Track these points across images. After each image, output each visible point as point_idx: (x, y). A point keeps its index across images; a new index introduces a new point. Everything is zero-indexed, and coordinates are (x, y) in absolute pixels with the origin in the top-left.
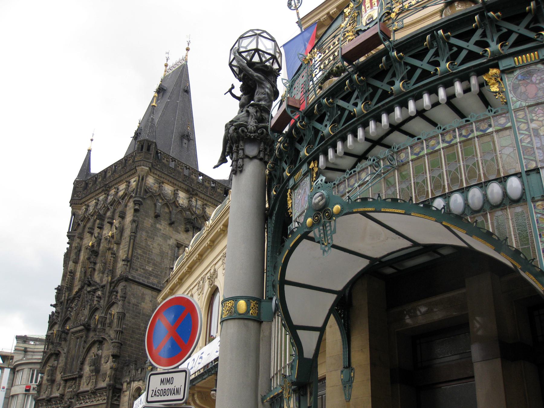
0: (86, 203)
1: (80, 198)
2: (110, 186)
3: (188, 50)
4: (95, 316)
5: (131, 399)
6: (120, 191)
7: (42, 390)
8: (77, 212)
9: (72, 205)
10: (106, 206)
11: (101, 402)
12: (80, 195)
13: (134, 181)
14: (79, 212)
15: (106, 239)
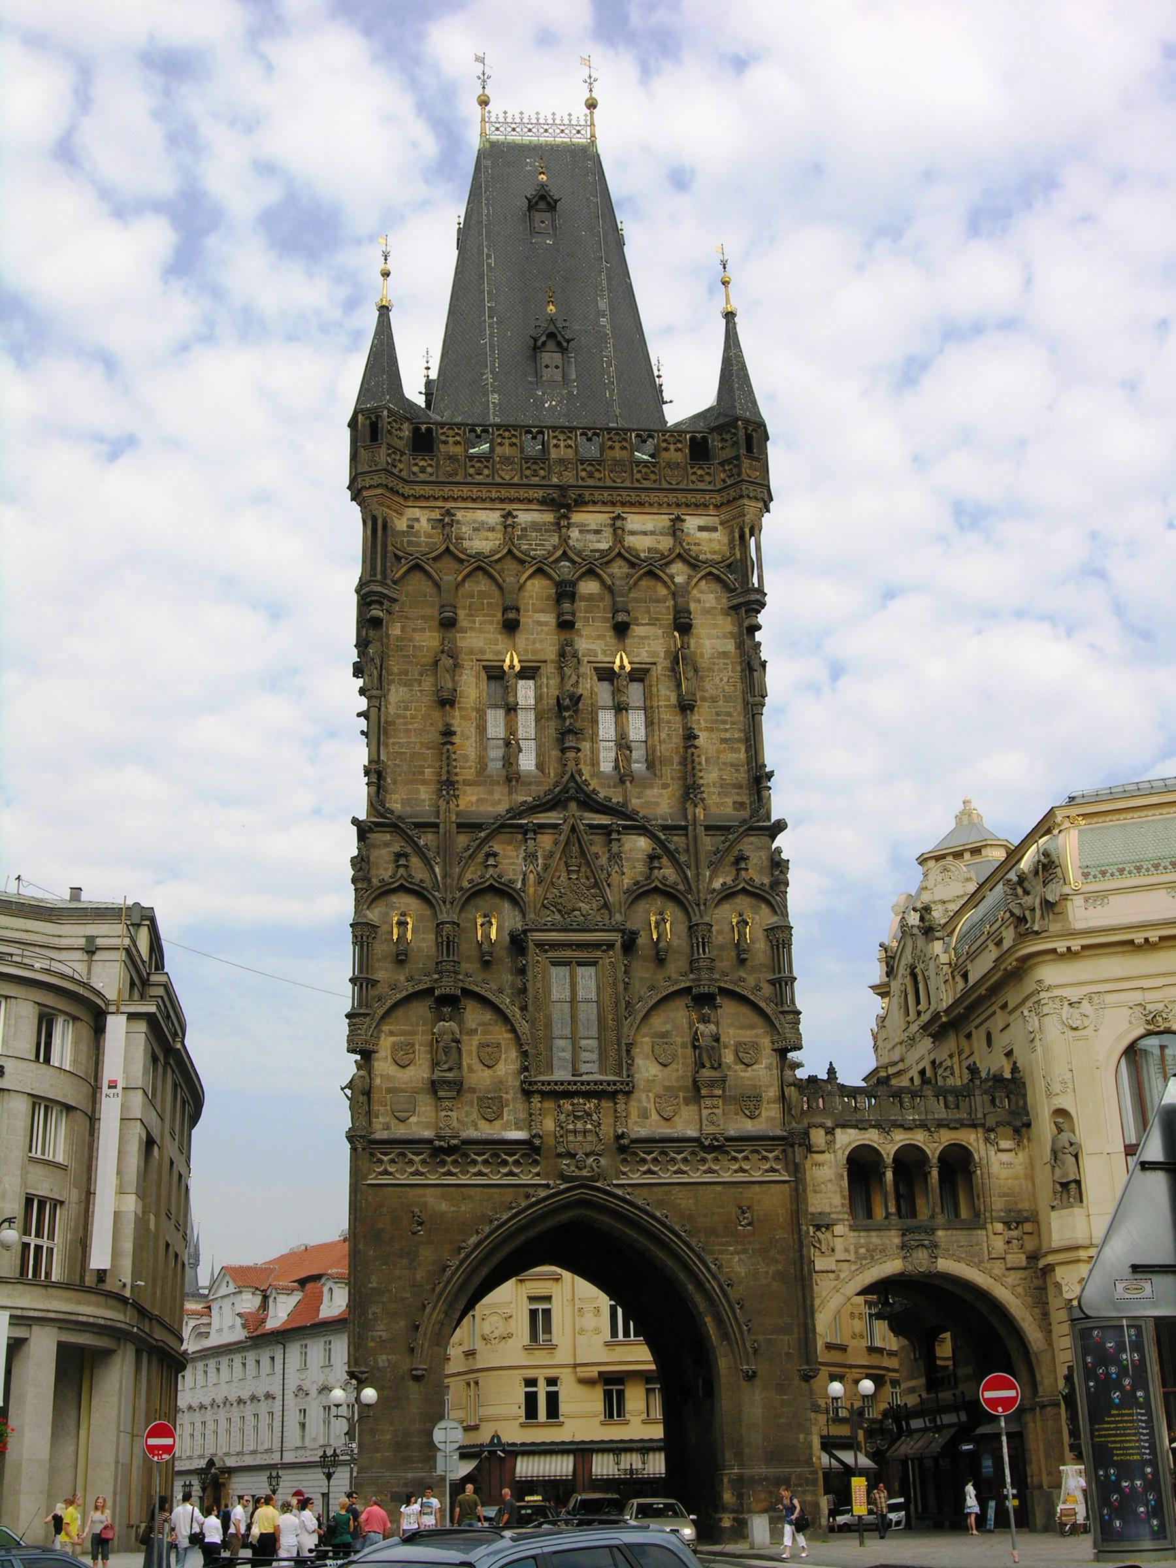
0: (449, 505)
1: (404, 474)
2: (587, 493)
3: (592, 105)
4: (661, 914)
5: (842, 1176)
6: (632, 533)
7: (376, 1108)
8: (392, 521)
9: (379, 491)
10: (579, 560)
11: (757, 1176)
12: (401, 466)
13: (701, 529)
14: (396, 521)
15: (606, 674)
